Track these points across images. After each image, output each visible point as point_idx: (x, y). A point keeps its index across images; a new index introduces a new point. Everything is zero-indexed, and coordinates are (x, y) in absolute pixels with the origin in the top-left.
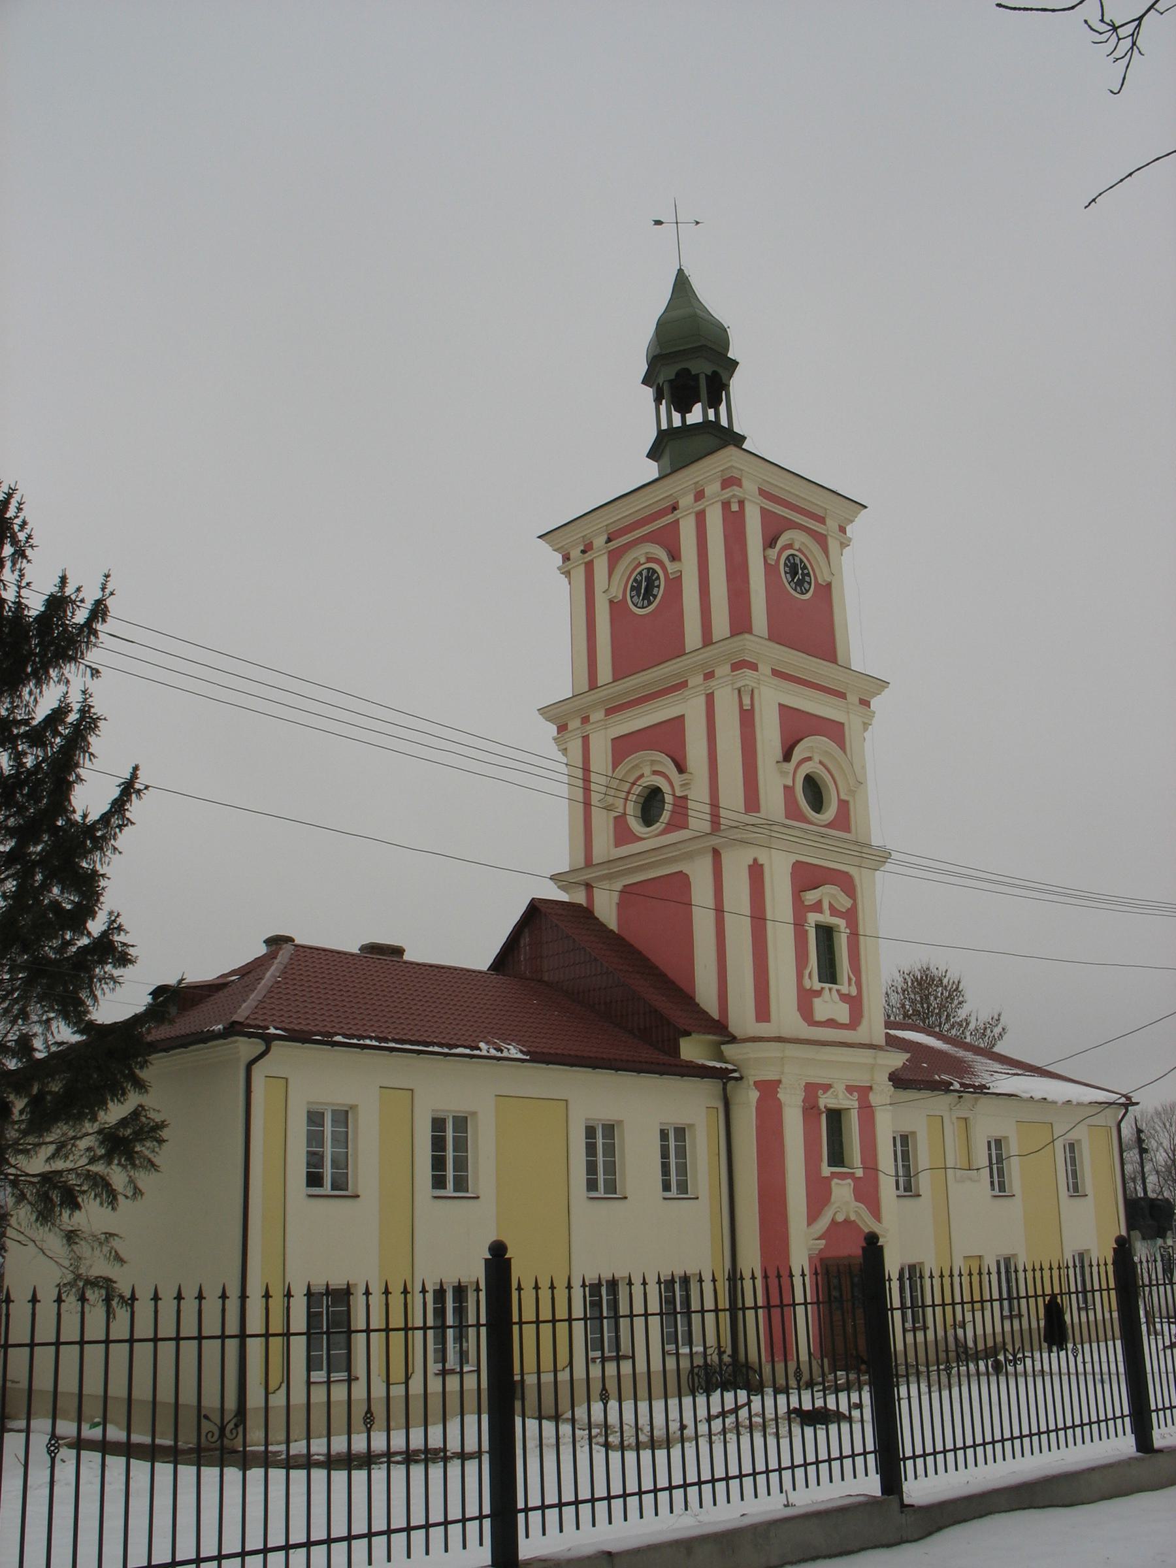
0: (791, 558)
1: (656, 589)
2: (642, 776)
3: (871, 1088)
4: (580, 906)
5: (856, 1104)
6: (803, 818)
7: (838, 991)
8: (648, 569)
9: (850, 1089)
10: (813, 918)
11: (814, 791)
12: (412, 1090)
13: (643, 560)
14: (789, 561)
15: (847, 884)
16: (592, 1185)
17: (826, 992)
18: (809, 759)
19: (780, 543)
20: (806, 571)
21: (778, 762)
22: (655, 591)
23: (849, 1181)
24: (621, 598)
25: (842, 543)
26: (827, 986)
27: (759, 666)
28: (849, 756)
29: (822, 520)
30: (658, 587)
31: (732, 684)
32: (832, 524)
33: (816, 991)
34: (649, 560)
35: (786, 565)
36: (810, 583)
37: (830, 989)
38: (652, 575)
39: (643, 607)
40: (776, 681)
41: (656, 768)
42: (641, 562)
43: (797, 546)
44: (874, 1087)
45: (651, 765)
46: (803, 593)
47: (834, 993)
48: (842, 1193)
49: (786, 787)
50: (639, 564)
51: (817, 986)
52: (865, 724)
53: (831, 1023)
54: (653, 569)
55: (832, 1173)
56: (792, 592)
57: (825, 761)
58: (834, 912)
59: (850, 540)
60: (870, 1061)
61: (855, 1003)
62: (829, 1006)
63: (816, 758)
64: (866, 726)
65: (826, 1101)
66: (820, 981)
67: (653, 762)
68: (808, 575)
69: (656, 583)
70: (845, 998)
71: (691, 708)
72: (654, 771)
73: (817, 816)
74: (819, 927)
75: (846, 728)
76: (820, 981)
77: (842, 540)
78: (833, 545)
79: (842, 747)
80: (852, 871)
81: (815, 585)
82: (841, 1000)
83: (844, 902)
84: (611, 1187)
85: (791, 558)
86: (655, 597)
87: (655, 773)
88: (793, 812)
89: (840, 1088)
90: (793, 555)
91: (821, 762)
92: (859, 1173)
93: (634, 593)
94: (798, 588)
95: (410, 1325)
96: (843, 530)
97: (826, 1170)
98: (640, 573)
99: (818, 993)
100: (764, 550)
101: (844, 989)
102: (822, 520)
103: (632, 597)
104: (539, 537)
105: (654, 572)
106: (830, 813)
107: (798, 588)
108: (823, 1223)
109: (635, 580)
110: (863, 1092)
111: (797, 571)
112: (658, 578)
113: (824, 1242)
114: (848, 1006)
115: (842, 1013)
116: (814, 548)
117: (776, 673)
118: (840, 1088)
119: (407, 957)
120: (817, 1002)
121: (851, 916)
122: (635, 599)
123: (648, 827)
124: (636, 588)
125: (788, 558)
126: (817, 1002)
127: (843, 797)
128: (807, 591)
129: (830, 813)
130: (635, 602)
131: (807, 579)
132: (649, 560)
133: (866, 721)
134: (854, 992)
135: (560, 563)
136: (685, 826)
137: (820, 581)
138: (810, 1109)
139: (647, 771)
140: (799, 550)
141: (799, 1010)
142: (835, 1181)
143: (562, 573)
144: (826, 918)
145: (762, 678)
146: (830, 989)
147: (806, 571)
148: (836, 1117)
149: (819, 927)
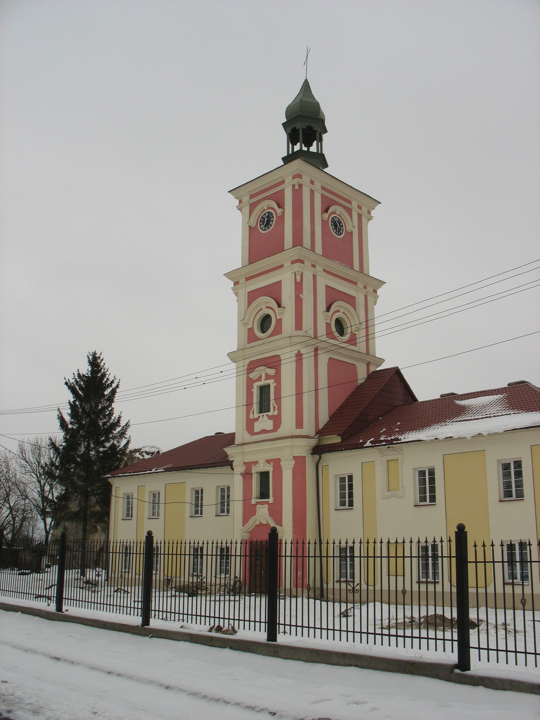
0: (335, 218)
1: (271, 222)
2: (262, 309)
6: (334, 338)
8: (269, 213)
11: (340, 325)
13: (266, 208)
14: (334, 220)
18: (338, 311)
19: (330, 211)
20: (341, 224)
22: (271, 224)
24: (255, 226)
27: (316, 266)
29: (350, 202)
30: (273, 221)
34: (269, 208)
36: (343, 230)
38: (271, 215)
39: (265, 230)
40: (324, 274)
42: (265, 209)
45: (266, 304)
46: (339, 235)
50: (264, 210)
54: (271, 213)
57: (345, 312)
63: (342, 311)
67: (266, 303)
68: (342, 226)
69: (272, 219)
72: (267, 307)
79: (355, 308)
85: (335, 218)
86: (271, 226)
87: (267, 307)
88: (329, 334)
91: (344, 313)
93: (261, 223)
95: (449, 558)
98: (265, 214)
102: (350, 202)
103: (260, 225)
105: (272, 214)
106: (347, 337)
109: (262, 218)
111: (337, 225)
116: (345, 214)
122: (262, 226)
124: (262, 221)
125: (333, 218)
128: (341, 234)
129: (347, 337)
130: (262, 227)
131: (342, 228)
132: (269, 208)
135: (238, 204)
139: (264, 307)
140: (339, 215)
143: (238, 209)
147: (341, 224)
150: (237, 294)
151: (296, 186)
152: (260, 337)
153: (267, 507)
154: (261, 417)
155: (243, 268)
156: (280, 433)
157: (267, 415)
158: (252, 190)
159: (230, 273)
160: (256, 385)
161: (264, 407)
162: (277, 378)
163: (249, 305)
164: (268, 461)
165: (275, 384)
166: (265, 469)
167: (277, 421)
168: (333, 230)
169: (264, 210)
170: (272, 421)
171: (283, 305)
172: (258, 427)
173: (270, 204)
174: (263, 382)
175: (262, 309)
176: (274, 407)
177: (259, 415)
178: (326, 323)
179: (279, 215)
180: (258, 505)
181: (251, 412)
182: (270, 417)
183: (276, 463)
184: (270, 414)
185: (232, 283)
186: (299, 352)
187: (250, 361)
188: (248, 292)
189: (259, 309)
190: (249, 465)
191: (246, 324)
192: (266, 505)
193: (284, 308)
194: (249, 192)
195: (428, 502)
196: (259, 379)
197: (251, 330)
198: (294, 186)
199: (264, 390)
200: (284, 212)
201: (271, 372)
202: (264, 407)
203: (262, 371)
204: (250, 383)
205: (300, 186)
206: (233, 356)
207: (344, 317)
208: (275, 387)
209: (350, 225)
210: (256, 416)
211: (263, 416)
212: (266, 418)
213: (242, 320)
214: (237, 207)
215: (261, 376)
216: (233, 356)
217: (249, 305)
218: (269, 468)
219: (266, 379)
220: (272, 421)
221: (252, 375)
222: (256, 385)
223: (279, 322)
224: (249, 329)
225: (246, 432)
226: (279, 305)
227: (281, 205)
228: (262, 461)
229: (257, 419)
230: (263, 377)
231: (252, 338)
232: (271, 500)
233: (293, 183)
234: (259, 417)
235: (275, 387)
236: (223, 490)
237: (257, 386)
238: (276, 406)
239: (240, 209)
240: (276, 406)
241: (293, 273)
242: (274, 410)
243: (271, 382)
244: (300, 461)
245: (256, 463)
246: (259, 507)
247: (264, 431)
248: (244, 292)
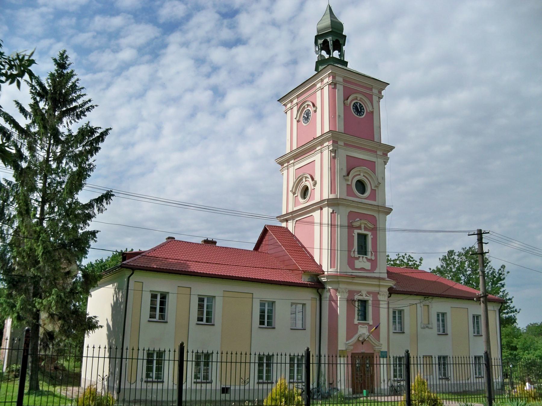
0: (356, 103)
3: (378, 293)
4: (284, 227)
5: (371, 299)
7: (366, 258)
8: (308, 110)
9: (369, 293)
10: (356, 231)
11: (361, 186)
12: (191, 288)
13: (306, 107)
14: (355, 104)
15: (374, 220)
16: (262, 323)
17: (361, 259)
18: (360, 175)
20: (362, 108)
21: (344, 176)
23: (367, 326)
25: (379, 97)
26: (361, 256)
28: (377, 175)
31: (329, 149)
32: (375, 91)
33: (357, 258)
35: (353, 106)
36: (364, 112)
37: (363, 257)
43: (359, 99)
44: (380, 293)
46: (360, 116)
47: (364, 258)
48: (363, 331)
49: (347, 185)
51: (357, 255)
52: (385, 162)
53: (363, 269)
55: (358, 323)
56: (356, 116)
58: (366, 229)
59: (383, 96)
60: (378, 283)
61: (374, 263)
62: (362, 263)
63: (362, 174)
64: (385, 163)
65: (357, 297)
66: (358, 254)
69: (310, 115)
70: (368, 260)
71: (317, 158)
73: (361, 195)
74: (359, 235)
75: (376, 163)
76: (358, 254)
77: (379, 96)
78: (375, 98)
80: (376, 215)
81: (366, 112)
82: (367, 261)
83: (370, 226)
84: (269, 324)
85: (356, 103)
89: (364, 293)
90: (357, 103)
91: (364, 176)
92: (371, 322)
94: (359, 114)
96: (380, 93)
97: (356, 322)
99: (358, 258)
100: (344, 101)
101: (369, 257)
103: (303, 120)
104: (278, 101)
107: (359, 114)
108: (354, 339)
110: (375, 295)
113: (352, 347)
114: (370, 263)
115: (368, 266)
117: (345, 144)
118: (364, 293)
119: (217, 245)
120: (356, 262)
121: (374, 230)
125: (354, 103)
126: (356, 262)
127: (373, 188)
128: (362, 115)
131: (363, 110)
133: (385, 161)
134: (373, 258)
136: (314, 199)
137: (368, 111)
138: (350, 301)
140: (360, 100)
141: (348, 264)
142: (360, 326)
144: (363, 232)
145: (339, 146)
146: (363, 257)
147: (362, 108)
148: (364, 303)
149: (359, 235)
168: (355, 112)
195: (204, 322)
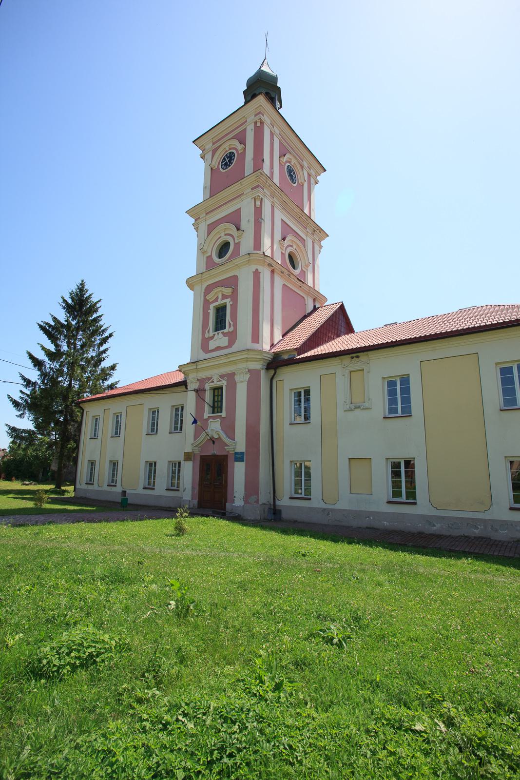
2: (221, 237)
8: (230, 153)
18: (292, 246)
30: (234, 159)
34: (230, 149)
39: (226, 169)
41: (226, 232)
50: (226, 151)
69: (233, 158)
87: (226, 235)
103: (221, 166)
105: (233, 153)
112: (234, 156)
123: (220, 258)
132: (230, 149)
139: (223, 235)
150: (197, 229)
151: (258, 123)
152: (217, 262)
153: (220, 421)
154: (216, 335)
155: (204, 202)
156: (235, 348)
157: (222, 333)
158: (214, 137)
159: (191, 210)
160: (212, 306)
161: (220, 324)
162: (234, 296)
163: (208, 235)
164: (222, 376)
165: (231, 303)
166: (219, 384)
167: (232, 337)
169: (226, 151)
170: (227, 338)
171: (242, 227)
172: (212, 345)
173: (232, 144)
174: (220, 302)
175: (221, 237)
176: (230, 324)
177: (214, 333)
178: (282, 253)
179: (240, 152)
180: (210, 420)
181: (207, 331)
182: (224, 334)
183: (231, 377)
184: (226, 331)
185: (193, 221)
186: (257, 270)
187: (207, 286)
188: (208, 225)
189: (219, 236)
190: (202, 381)
191: (204, 253)
192: (218, 419)
193: (243, 231)
194: (212, 139)
196: (216, 300)
197: (209, 258)
198: (256, 123)
199: (221, 311)
200: (245, 149)
201: (228, 291)
202: (220, 324)
203: (218, 292)
204: (206, 303)
205: (262, 123)
206: (191, 283)
207: (295, 252)
208: (231, 305)
209: (302, 175)
210: (211, 334)
211: (218, 334)
212: (221, 335)
213: (201, 250)
214: (200, 155)
215: (218, 297)
216: (191, 283)
217: (208, 235)
218: (224, 383)
219: (222, 299)
220: (227, 338)
221: (208, 297)
222: (212, 306)
223: (238, 245)
224: (207, 258)
225: (201, 351)
226: (238, 229)
227: (243, 142)
228: (215, 379)
229: (212, 338)
230: (220, 297)
231: (210, 265)
232: (224, 414)
233: (254, 121)
234: (214, 335)
235: (231, 305)
236: (177, 410)
237: (214, 307)
238: (232, 323)
239: (203, 157)
240: (232, 323)
241: (252, 198)
242: (230, 327)
243: (228, 302)
244: (254, 375)
245: (209, 379)
246: (211, 421)
247: (219, 348)
248: (203, 227)
